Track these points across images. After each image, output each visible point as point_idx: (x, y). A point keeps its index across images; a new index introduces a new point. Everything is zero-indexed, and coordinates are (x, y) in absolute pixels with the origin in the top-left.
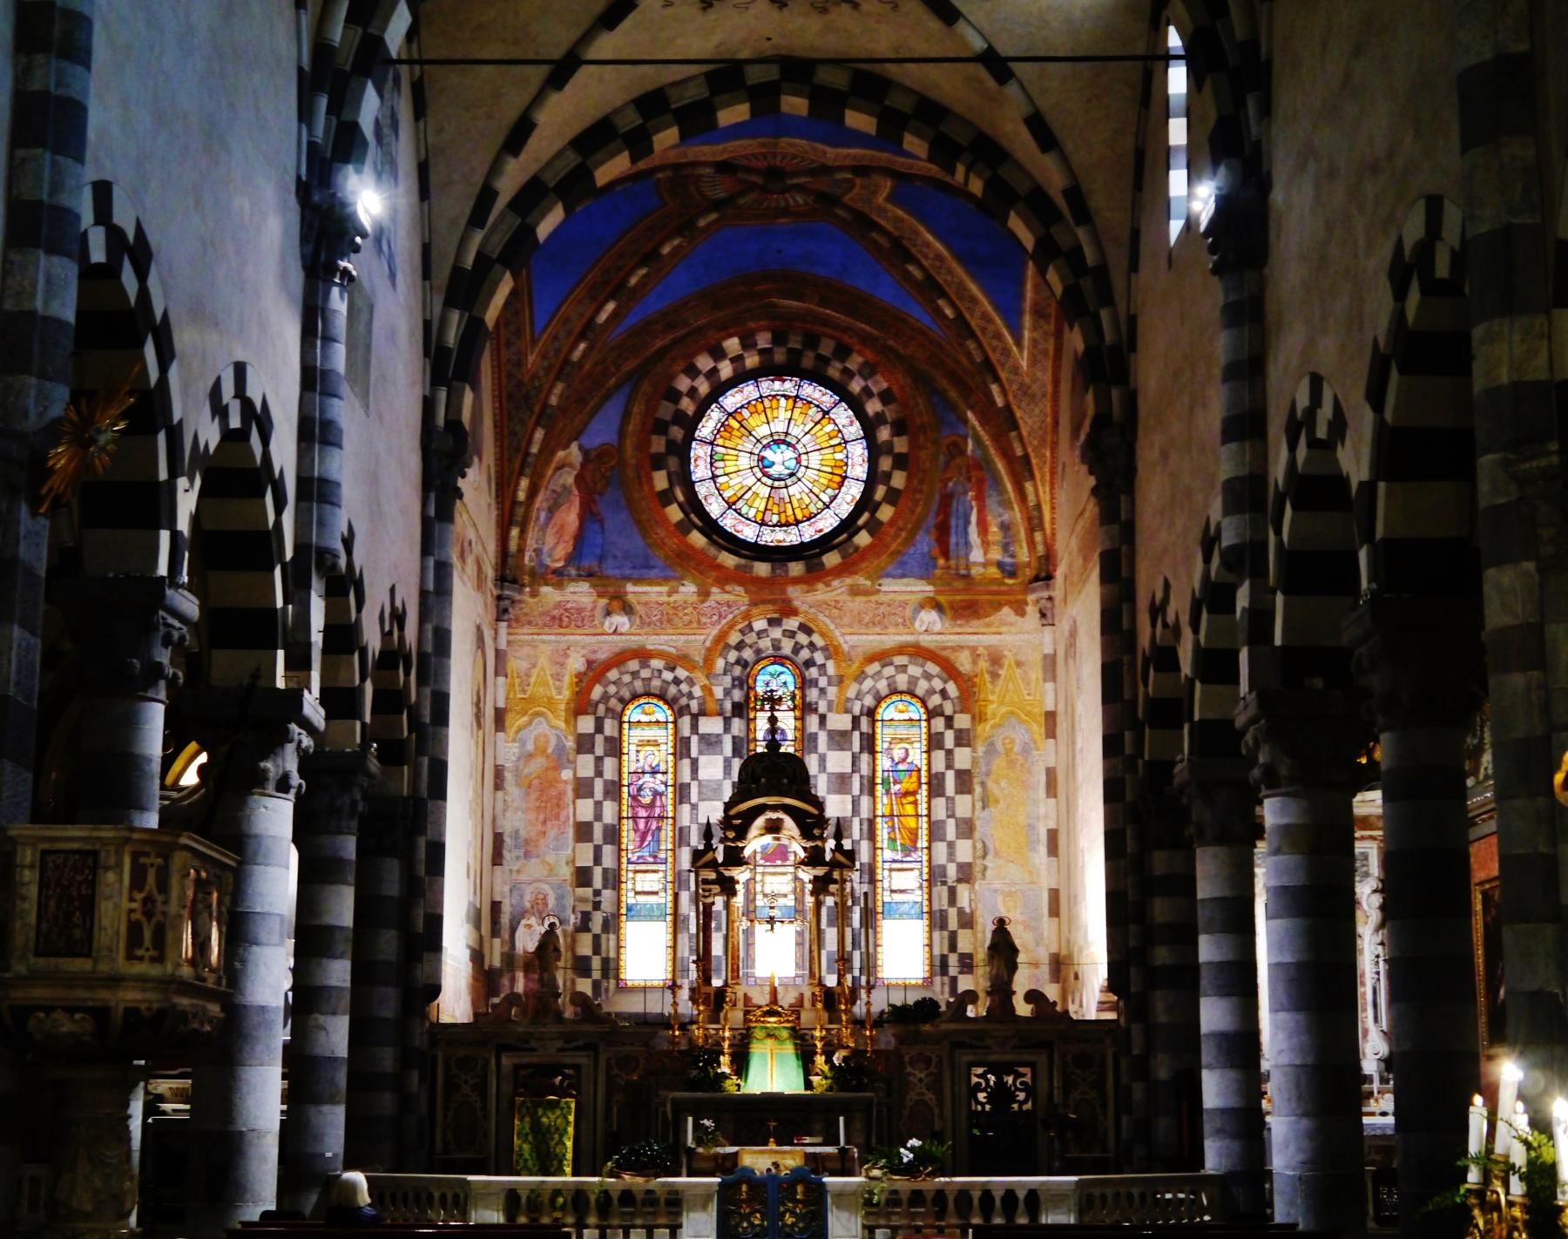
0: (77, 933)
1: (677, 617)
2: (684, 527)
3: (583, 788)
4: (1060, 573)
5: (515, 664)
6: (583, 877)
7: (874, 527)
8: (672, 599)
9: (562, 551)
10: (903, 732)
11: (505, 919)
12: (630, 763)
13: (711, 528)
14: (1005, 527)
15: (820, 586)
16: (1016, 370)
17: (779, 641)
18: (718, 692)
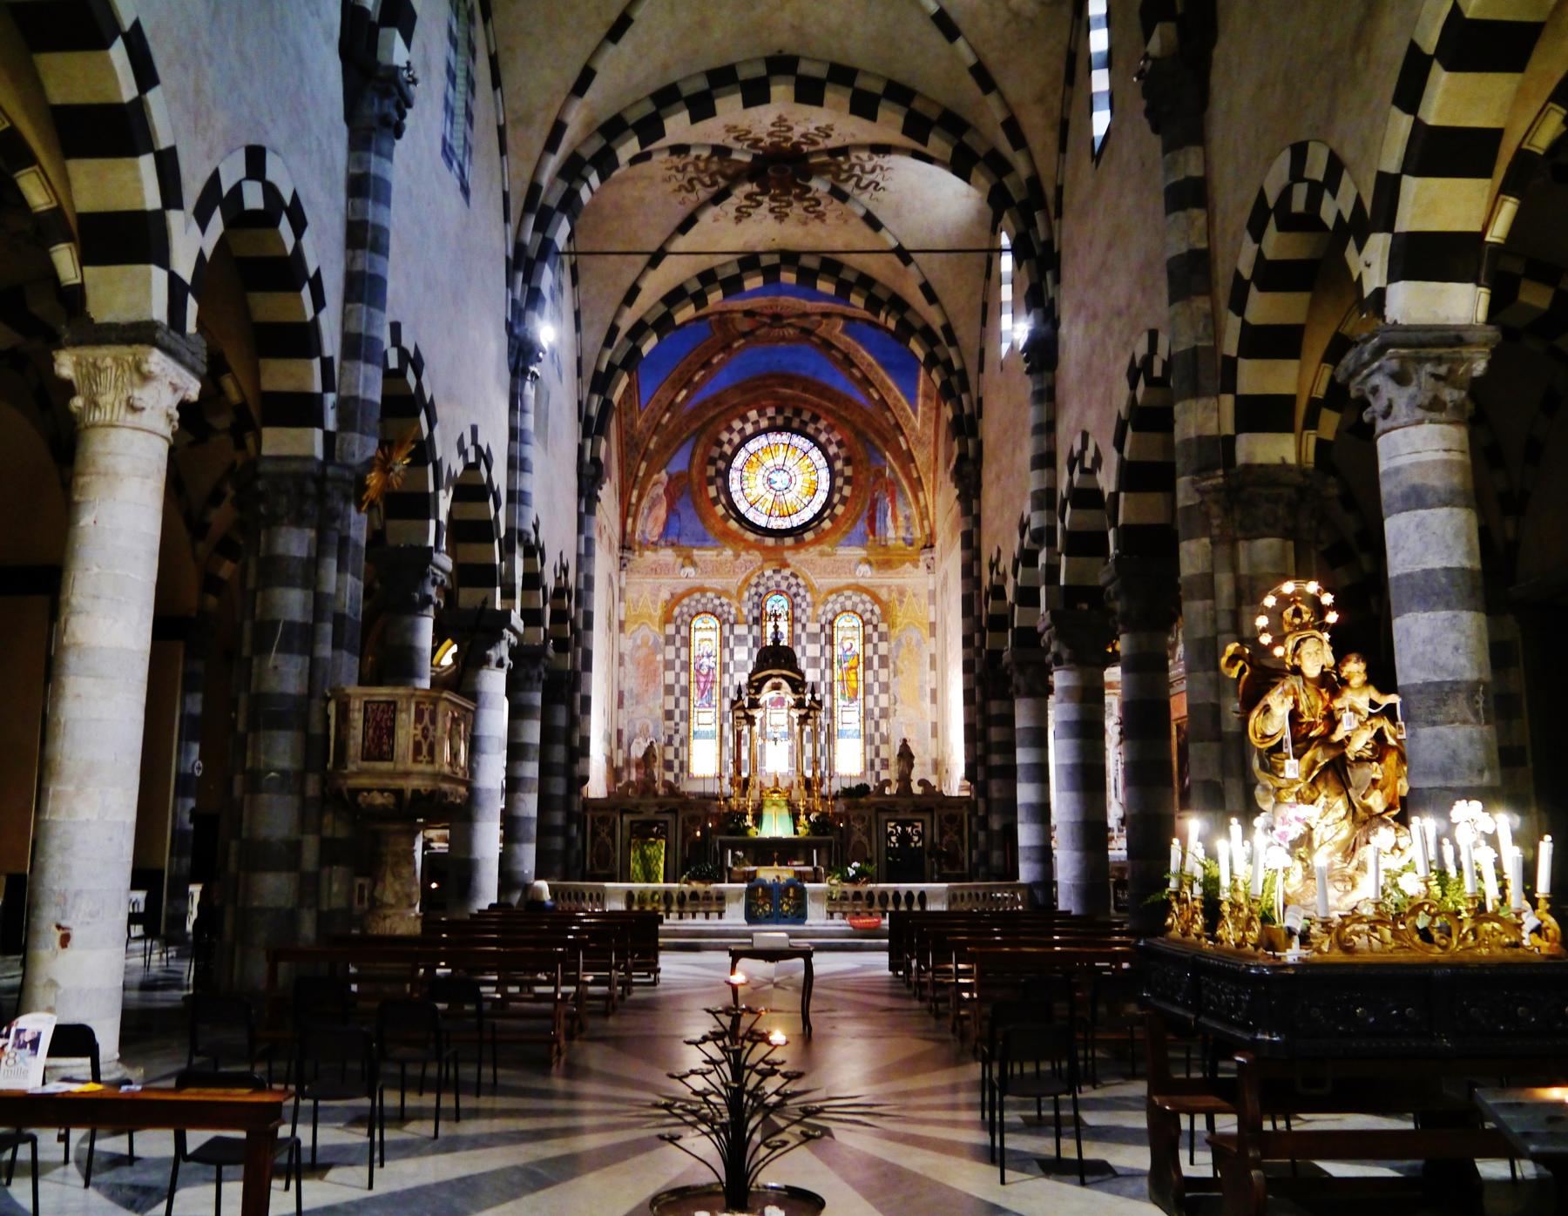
0: (385, 748)
1: (722, 569)
2: (726, 518)
3: (669, 665)
4: (938, 544)
5: (631, 595)
6: (669, 715)
7: (833, 518)
9: (658, 529)
10: (849, 634)
11: (625, 740)
12: (695, 651)
13: (741, 518)
14: (907, 518)
16: (913, 429)
18: (745, 611)
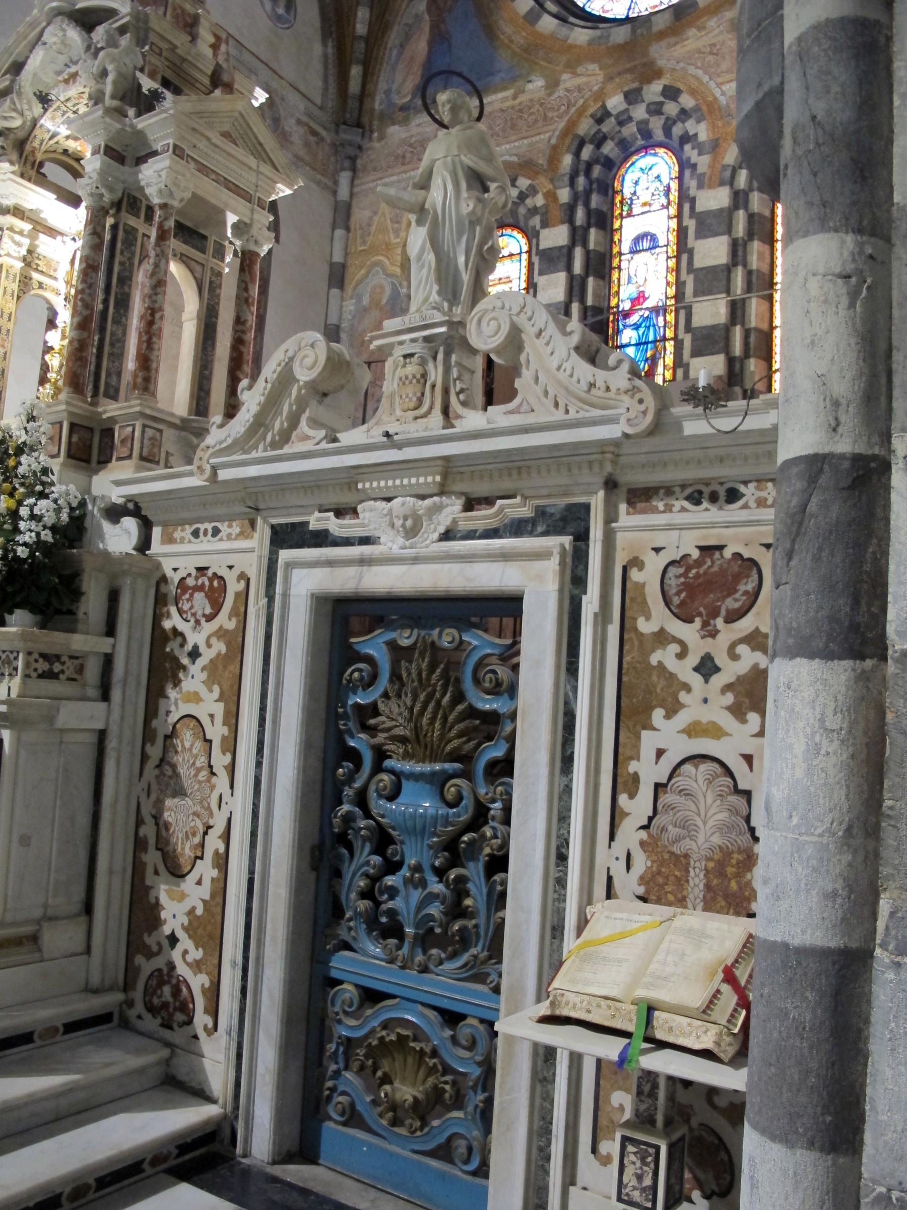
5: (359, 215)
8: (518, 101)
15: (692, 32)
17: (646, 122)
